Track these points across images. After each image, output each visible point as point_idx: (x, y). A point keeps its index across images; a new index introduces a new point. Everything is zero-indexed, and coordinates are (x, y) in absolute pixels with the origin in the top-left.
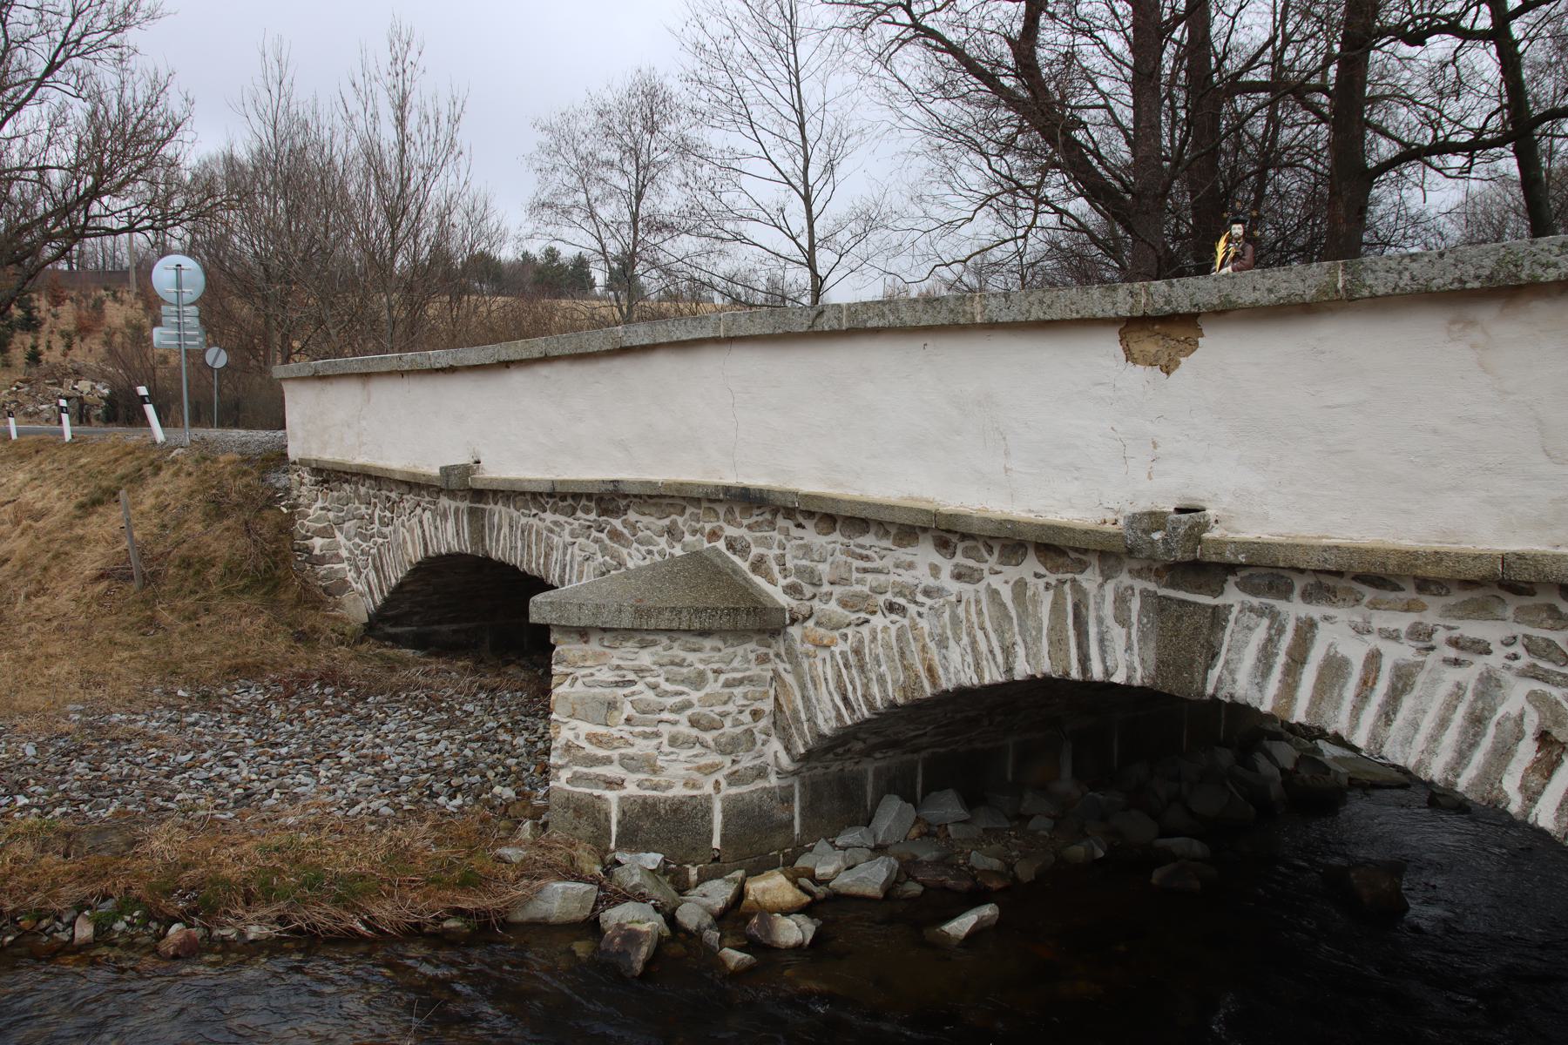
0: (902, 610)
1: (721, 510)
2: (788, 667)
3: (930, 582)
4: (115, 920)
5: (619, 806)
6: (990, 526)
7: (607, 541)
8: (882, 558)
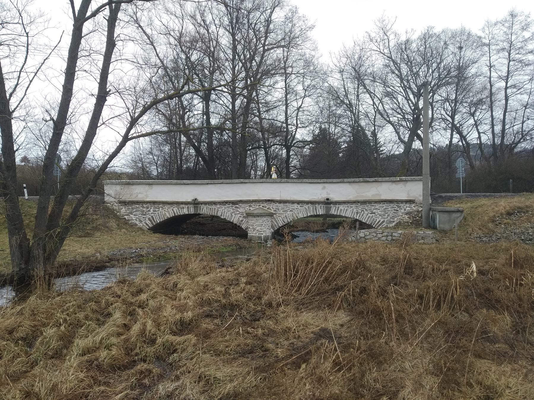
1: (261, 203)
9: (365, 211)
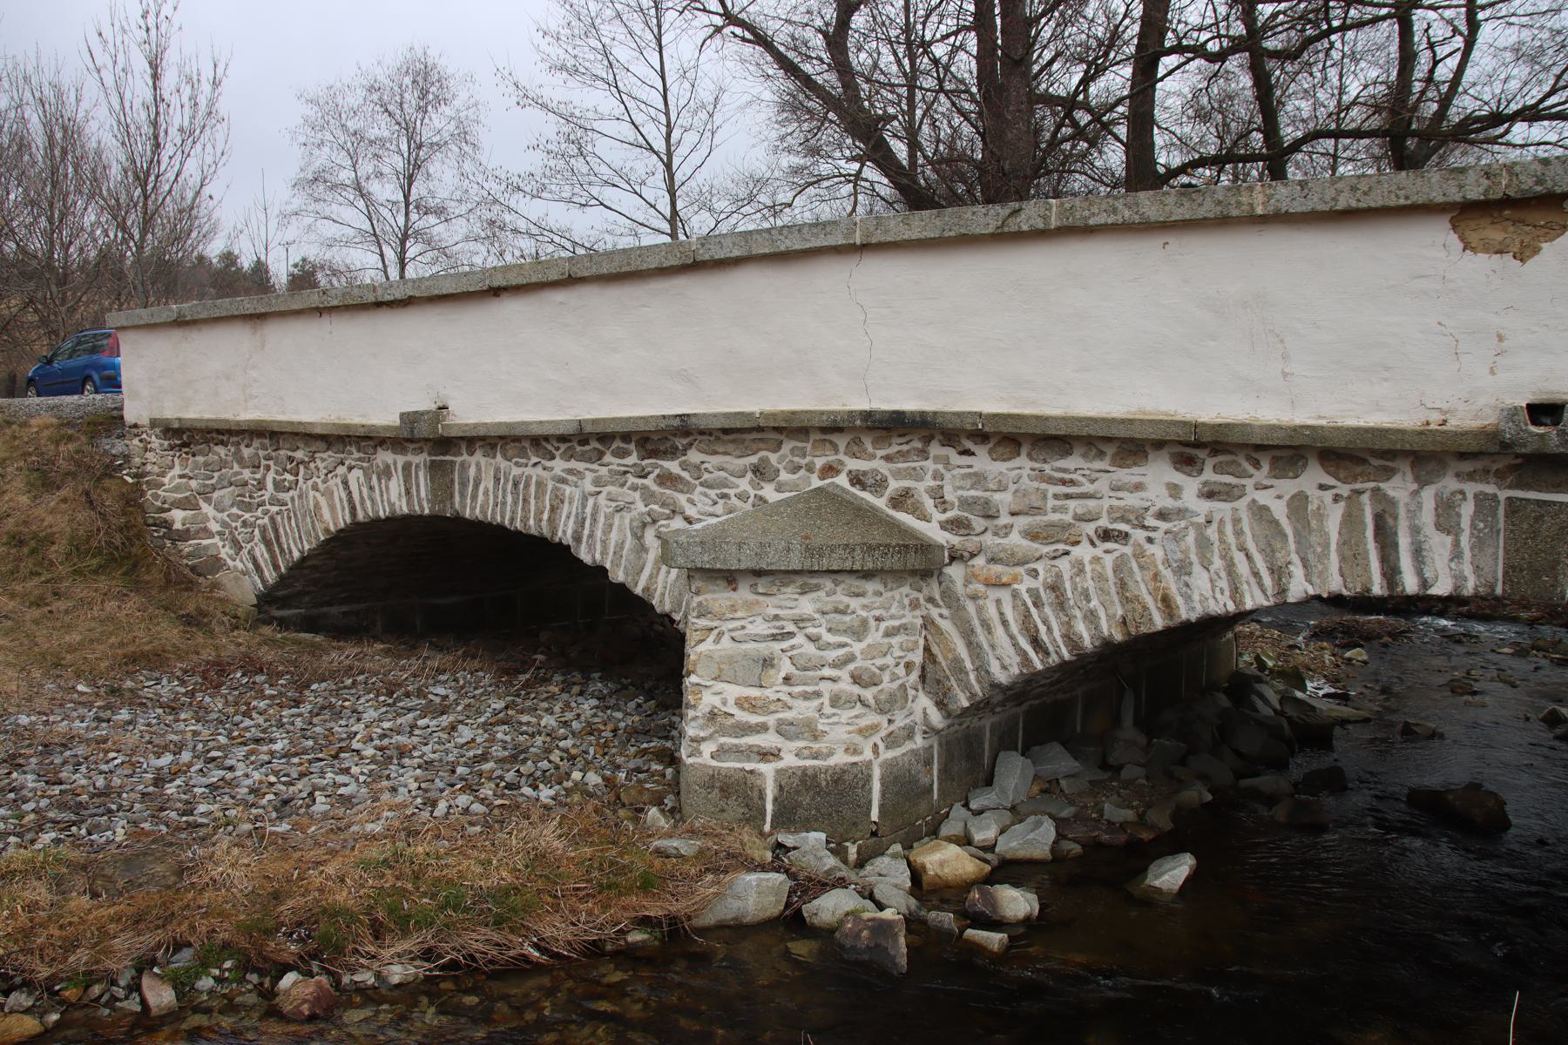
0: (1124, 537)
1: (842, 441)
2: (945, 612)
3: (1170, 503)
4: (198, 977)
5: (776, 780)
6: (1281, 434)
7: (655, 488)
8: (1093, 481)
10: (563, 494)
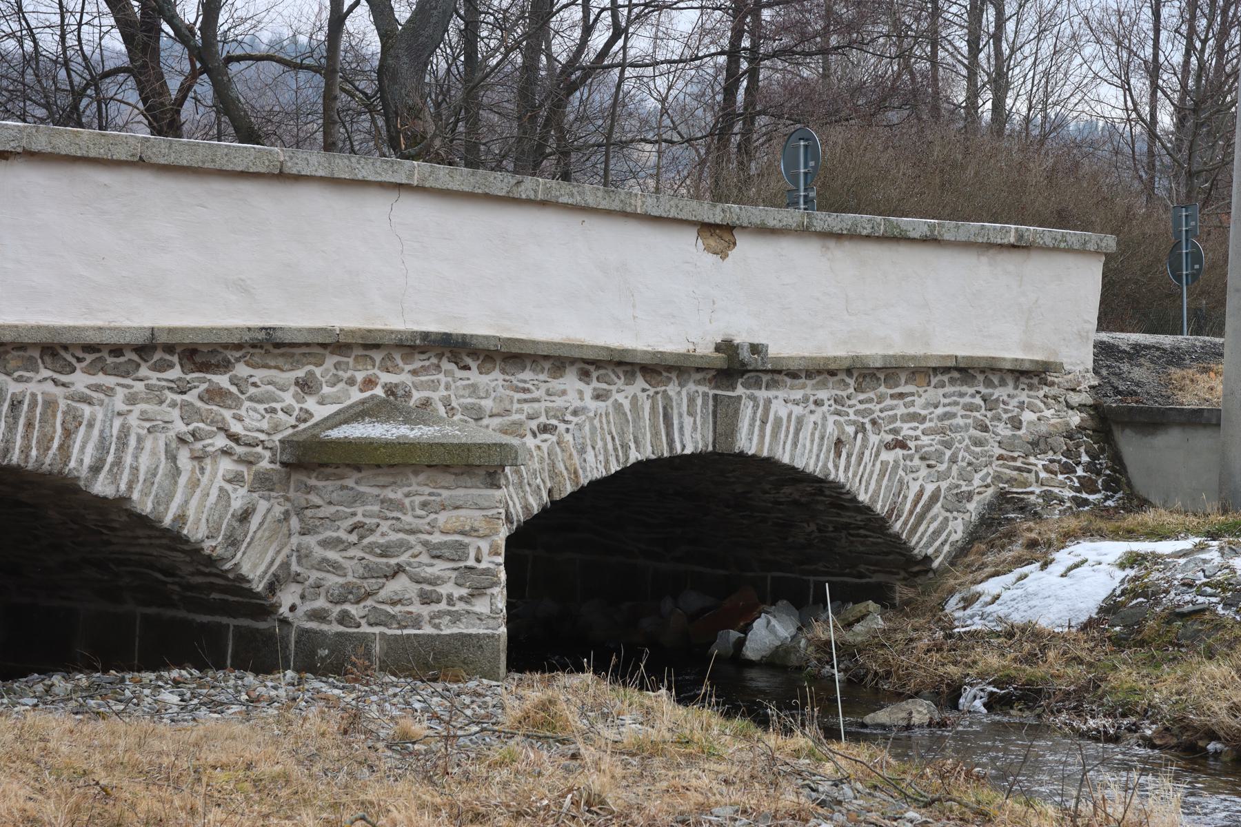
1: (378, 356)
3: (577, 404)
9: (869, 426)
10: (82, 416)
